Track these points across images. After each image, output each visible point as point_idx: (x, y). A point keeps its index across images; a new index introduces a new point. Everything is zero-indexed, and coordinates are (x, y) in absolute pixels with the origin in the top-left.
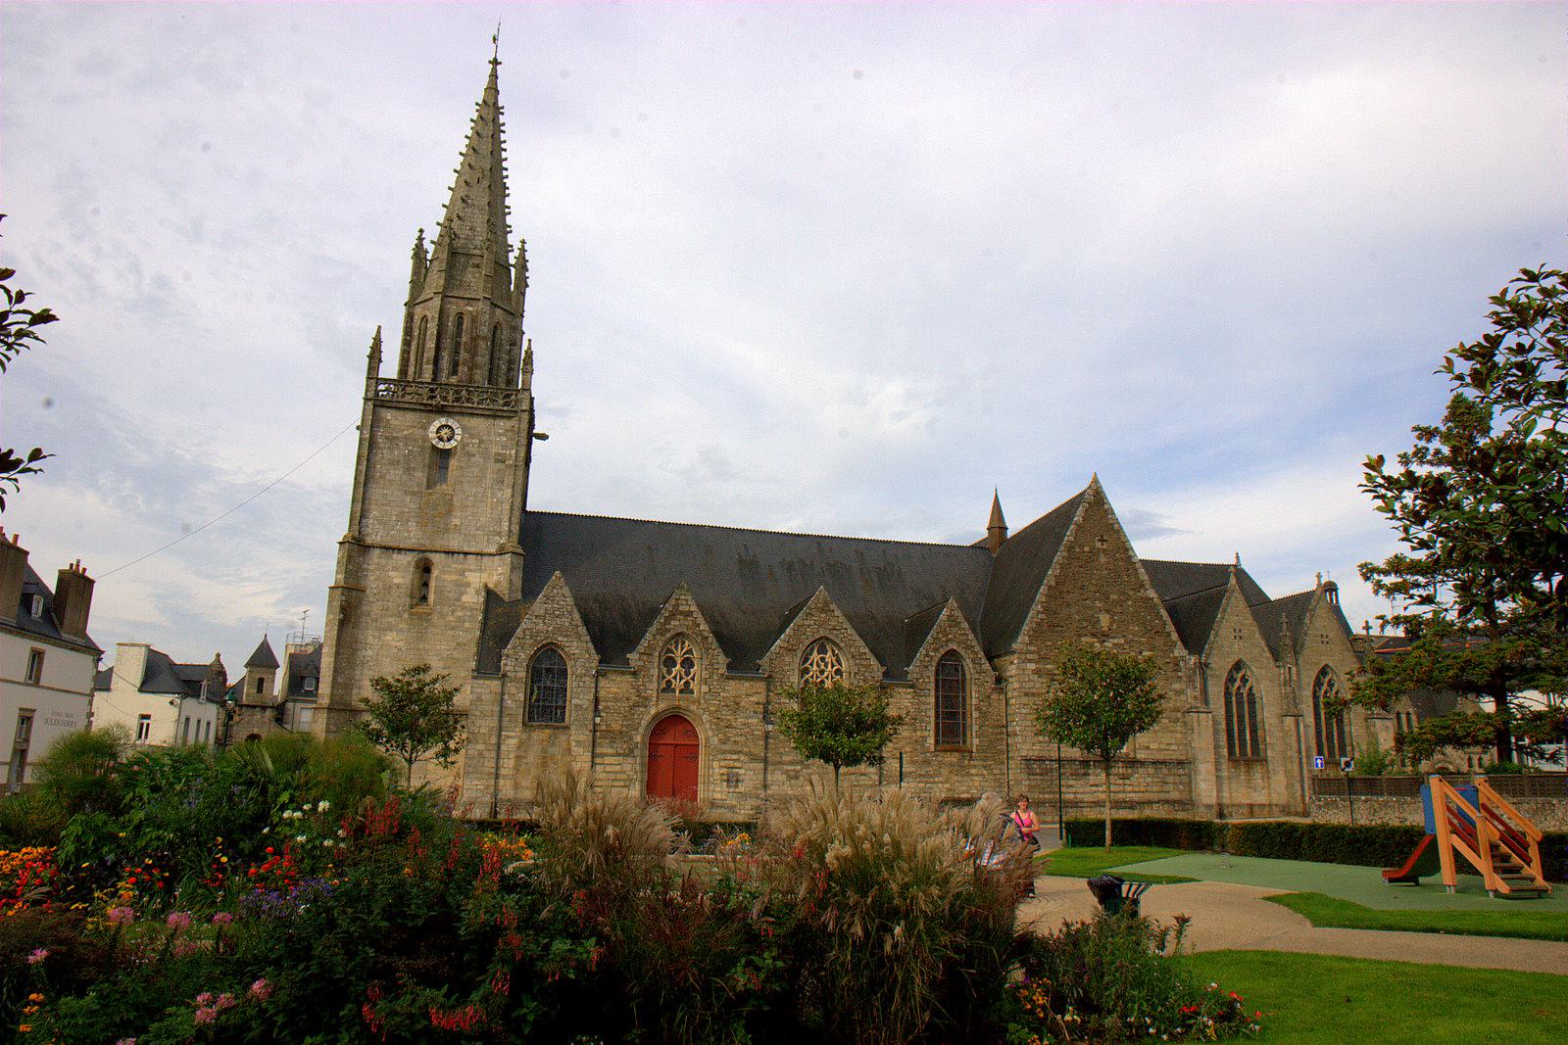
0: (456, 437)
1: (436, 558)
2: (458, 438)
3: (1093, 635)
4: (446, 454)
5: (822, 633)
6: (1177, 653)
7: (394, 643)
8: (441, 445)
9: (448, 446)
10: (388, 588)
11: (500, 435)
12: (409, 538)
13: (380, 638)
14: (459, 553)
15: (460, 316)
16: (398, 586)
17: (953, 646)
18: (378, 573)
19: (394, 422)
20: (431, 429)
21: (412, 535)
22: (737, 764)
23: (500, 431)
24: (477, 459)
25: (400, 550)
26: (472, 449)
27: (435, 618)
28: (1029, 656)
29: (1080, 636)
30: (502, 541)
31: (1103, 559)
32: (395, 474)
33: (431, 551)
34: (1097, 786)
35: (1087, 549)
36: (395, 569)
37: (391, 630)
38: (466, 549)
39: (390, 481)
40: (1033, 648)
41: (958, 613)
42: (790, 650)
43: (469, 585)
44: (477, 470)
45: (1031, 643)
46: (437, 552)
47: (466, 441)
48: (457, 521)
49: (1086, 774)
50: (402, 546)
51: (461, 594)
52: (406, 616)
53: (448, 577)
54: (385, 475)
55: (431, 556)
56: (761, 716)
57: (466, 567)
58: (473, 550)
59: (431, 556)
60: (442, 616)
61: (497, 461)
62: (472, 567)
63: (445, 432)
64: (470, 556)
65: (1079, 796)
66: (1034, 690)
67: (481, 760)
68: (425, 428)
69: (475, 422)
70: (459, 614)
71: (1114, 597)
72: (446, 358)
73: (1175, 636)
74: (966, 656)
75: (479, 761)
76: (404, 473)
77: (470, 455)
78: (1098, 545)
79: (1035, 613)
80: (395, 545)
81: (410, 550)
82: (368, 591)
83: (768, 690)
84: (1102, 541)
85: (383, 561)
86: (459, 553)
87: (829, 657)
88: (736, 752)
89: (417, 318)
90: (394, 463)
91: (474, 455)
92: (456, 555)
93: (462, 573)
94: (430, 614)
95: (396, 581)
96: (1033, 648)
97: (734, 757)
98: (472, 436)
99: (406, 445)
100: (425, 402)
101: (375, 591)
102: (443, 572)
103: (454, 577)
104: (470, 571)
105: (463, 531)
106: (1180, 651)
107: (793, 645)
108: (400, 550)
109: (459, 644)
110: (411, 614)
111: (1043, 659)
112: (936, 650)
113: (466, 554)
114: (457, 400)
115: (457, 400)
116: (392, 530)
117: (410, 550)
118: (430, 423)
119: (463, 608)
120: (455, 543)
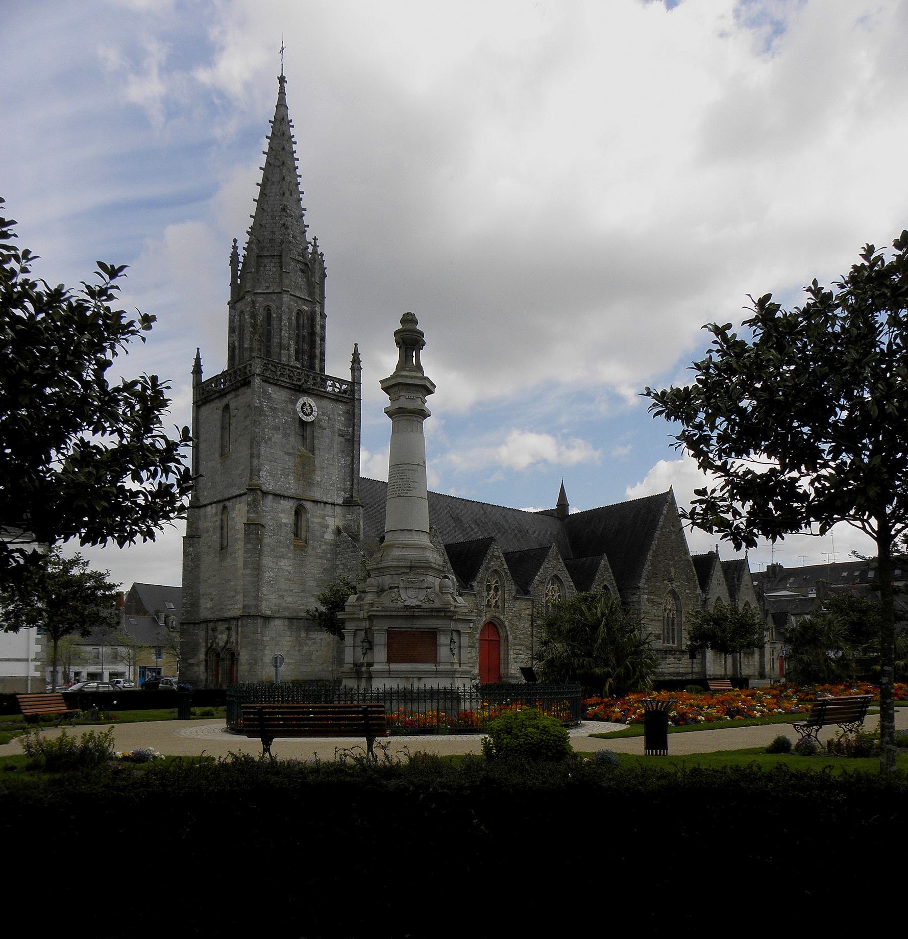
1: (308, 505)
2: (315, 414)
3: (669, 580)
4: (303, 423)
5: (555, 573)
6: (697, 592)
7: (286, 568)
8: (304, 418)
9: (310, 419)
10: (280, 526)
11: (340, 415)
12: (290, 489)
13: (277, 563)
14: (321, 502)
15: (299, 313)
16: (286, 524)
17: (606, 583)
18: (272, 514)
19: (273, 396)
20: (298, 405)
21: (291, 486)
22: (521, 652)
23: (340, 412)
24: (327, 432)
25: (285, 497)
27: (309, 549)
28: (645, 591)
29: (664, 580)
30: (346, 496)
31: (673, 537)
32: (278, 437)
33: (305, 500)
34: (669, 664)
35: (667, 530)
36: (283, 511)
37: (283, 558)
39: (275, 443)
40: (647, 586)
41: (608, 564)
42: (542, 582)
43: (327, 526)
45: (645, 584)
46: (308, 500)
48: (318, 479)
49: (666, 658)
50: (286, 494)
51: (324, 533)
52: (292, 547)
53: (316, 520)
55: (304, 503)
56: (530, 623)
57: (326, 513)
58: (329, 501)
59: (304, 503)
60: (314, 549)
61: (340, 435)
62: (329, 514)
64: (327, 505)
65: (663, 670)
66: (647, 610)
68: (294, 402)
69: (326, 403)
70: (324, 547)
71: (676, 558)
73: (697, 582)
74: (610, 589)
76: (283, 437)
77: (321, 427)
78: (672, 527)
79: (647, 567)
80: (281, 493)
81: (292, 498)
82: (267, 527)
83: (533, 607)
84: (673, 526)
85: (275, 505)
86: (321, 502)
87: (555, 586)
88: (521, 645)
91: (325, 429)
93: (323, 517)
94: (306, 547)
95: (284, 521)
96: (647, 586)
97: (520, 647)
98: (323, 414)
99: (283, 415)
100: (294, 382)
101: (272, 528)
102: (313, 516)
103: (319, 520)
104: (328, 516)
106: (699, 591)
107: (543, 579)
108: (285, 497)
109: (324, 570)
110: (295, 546)
111: (650, 593)
112: (599, 585)
113: (325, 503)
114: (314, 384)
115: (314, 384)
117: (292, 498)
118: (297, 401)
119: (326, 543)
120: (318, 495)
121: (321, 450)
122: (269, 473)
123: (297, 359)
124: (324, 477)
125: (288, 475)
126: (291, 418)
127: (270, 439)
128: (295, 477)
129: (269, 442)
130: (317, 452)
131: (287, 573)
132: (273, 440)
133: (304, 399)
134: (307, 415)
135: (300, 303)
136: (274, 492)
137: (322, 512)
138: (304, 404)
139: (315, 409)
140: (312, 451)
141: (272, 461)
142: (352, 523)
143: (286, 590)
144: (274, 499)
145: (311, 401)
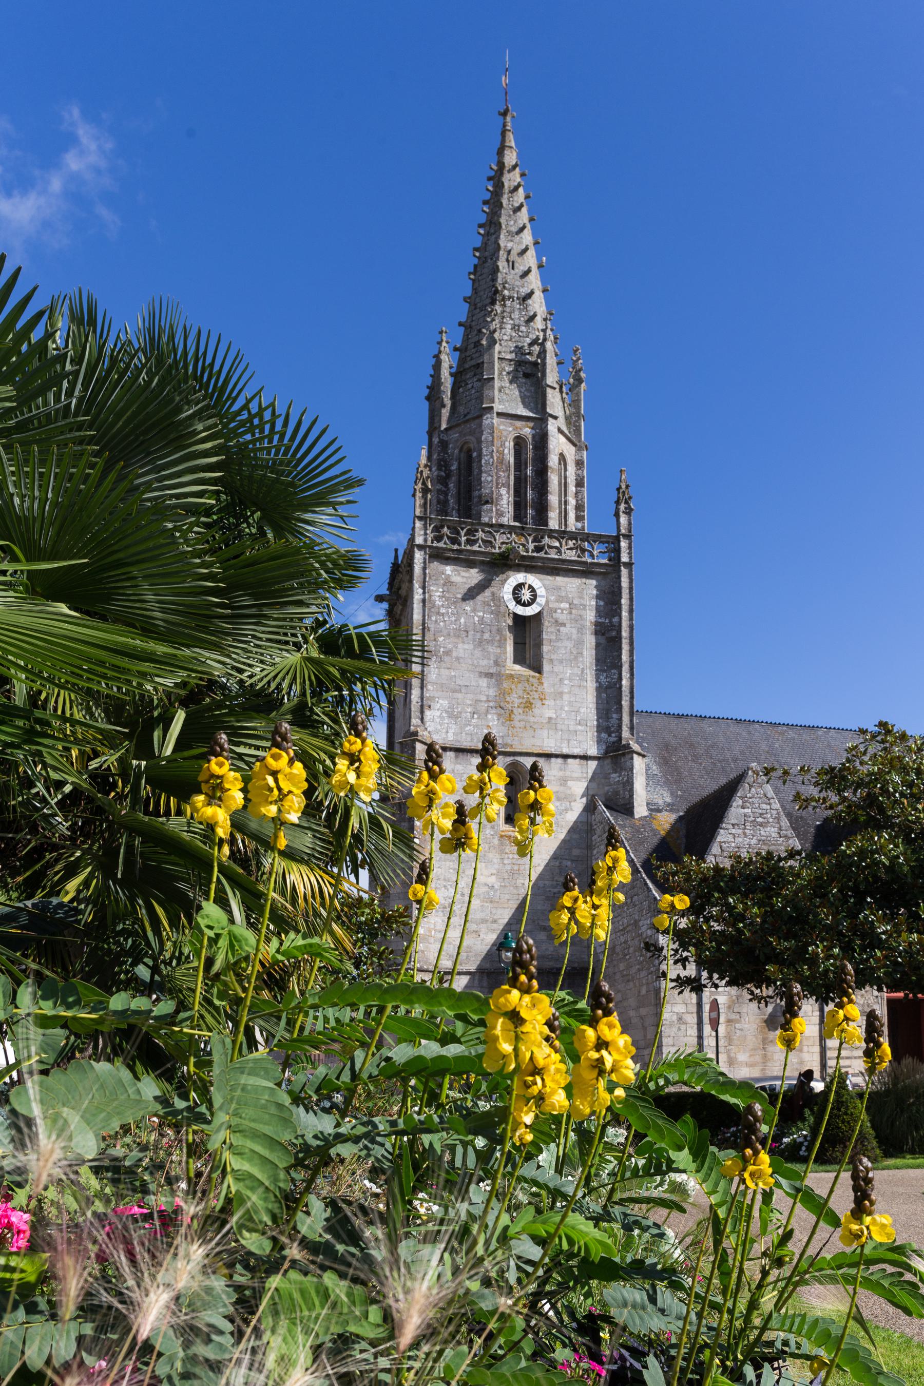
0: (538, 600)
8: (521, 611)
14: (557, 756)
15: (519, 442)
19: (456, 579)
26: (562, 617)
32: (464, 649)
38: (565, 751)
39: (458, 659)
44: (569, 644)
47: (551, 606)
48: (550, 713)
54: (451, 651)
57: (568, 773)
58: (576, 751)
62: (575, 775)
63: (526, 595)
64: (570, 761)
67: (683, 1027)
69: (560, 580)
72: (505, 497)
75: (679, 1029)
86: (557, 756)
89: (454, 451)
90: (462, 633)
91: (564, 625)
92: (553, 760)
98: (560, 599)
99: (474, 610)
104: (573, 779)
105: (559, 727)
113: (566, 757)
116: (467, 725)
121: (555, 663)
122: (447, 712)
123: (517, 518)
124: (562, 708)
125: (487, 712)
126: (492, 613)
127: (448, 653)
128: (499, 715)
129: (446, 659)
130: (546, 667)
131: (485, 889)
132: (454, 654)
133: (517, 578)
134: (524, 605)
135: (519, 424)
136: (458, 745)
137: (561, 773)
138: (519, 587)
139: (541, 591)
140: (538, 669)
141: (454, 691)
142: (620, 788)
143: (484, 921)
144: (457, 757)
145: (532, 579)
